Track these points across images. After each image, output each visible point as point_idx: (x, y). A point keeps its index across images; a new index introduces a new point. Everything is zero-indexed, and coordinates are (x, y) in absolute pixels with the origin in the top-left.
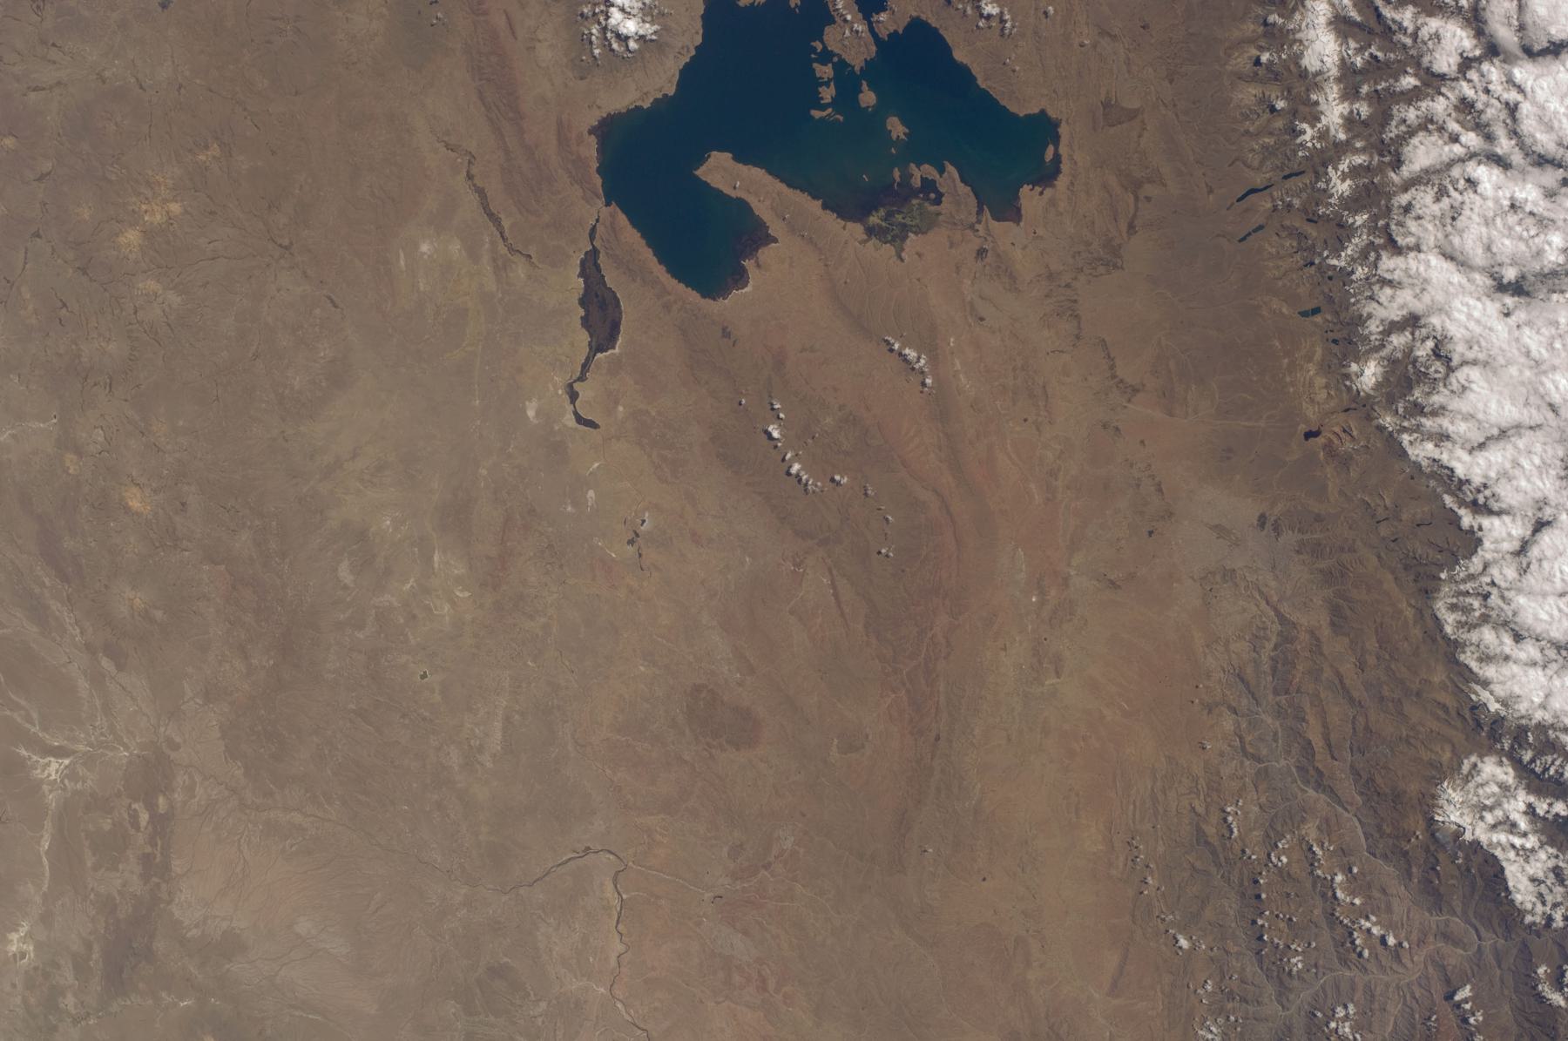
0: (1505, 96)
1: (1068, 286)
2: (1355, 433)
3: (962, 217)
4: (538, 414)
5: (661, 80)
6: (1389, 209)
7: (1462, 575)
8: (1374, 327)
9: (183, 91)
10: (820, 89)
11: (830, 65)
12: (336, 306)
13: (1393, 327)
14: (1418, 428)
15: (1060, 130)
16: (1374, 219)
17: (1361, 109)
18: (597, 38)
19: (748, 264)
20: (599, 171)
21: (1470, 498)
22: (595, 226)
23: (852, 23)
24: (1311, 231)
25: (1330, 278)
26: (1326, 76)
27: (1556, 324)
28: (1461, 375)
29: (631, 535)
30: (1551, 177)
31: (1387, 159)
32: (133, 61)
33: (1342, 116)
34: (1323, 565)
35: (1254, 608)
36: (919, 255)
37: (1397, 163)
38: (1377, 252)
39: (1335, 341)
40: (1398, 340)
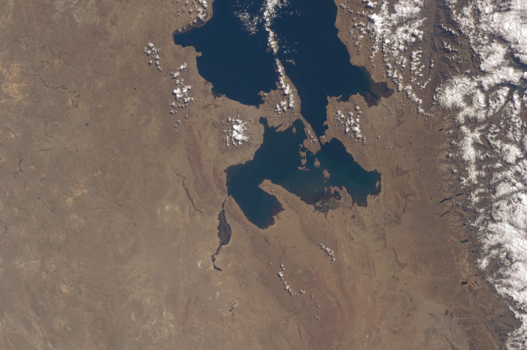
1: (382, 229)
2: (479, 283)
3: (347, 204)
4: (202, 265)
5: (249, 155)
6: (491, 208)
7: (515, 334)
8: (486, 247)
9: (91, 152)
10: (301, 160)
11: (305, 152)
12: (136, 226)
13: (492, 247)
14: (501, 283)
16: (486, 210)
17: (482, 173)
18: (228, 140)
19: (275, 217)
20: (226, 184)
21: (518, 307)
22: (224, 203)
23: (313, 138)
24: (465, 213)
25: (471, 230)
26: (471, 162)
28: (516, 265)
29: (231, 308)
31: (491, 191)
32: (75, 142)
33: (476, 176)
34: (467, 329)
35: (443, 343)
36: (332, 217)
37: (494, 192)
38: (487, 222)
39: (472, 252)
40: (494, 252)
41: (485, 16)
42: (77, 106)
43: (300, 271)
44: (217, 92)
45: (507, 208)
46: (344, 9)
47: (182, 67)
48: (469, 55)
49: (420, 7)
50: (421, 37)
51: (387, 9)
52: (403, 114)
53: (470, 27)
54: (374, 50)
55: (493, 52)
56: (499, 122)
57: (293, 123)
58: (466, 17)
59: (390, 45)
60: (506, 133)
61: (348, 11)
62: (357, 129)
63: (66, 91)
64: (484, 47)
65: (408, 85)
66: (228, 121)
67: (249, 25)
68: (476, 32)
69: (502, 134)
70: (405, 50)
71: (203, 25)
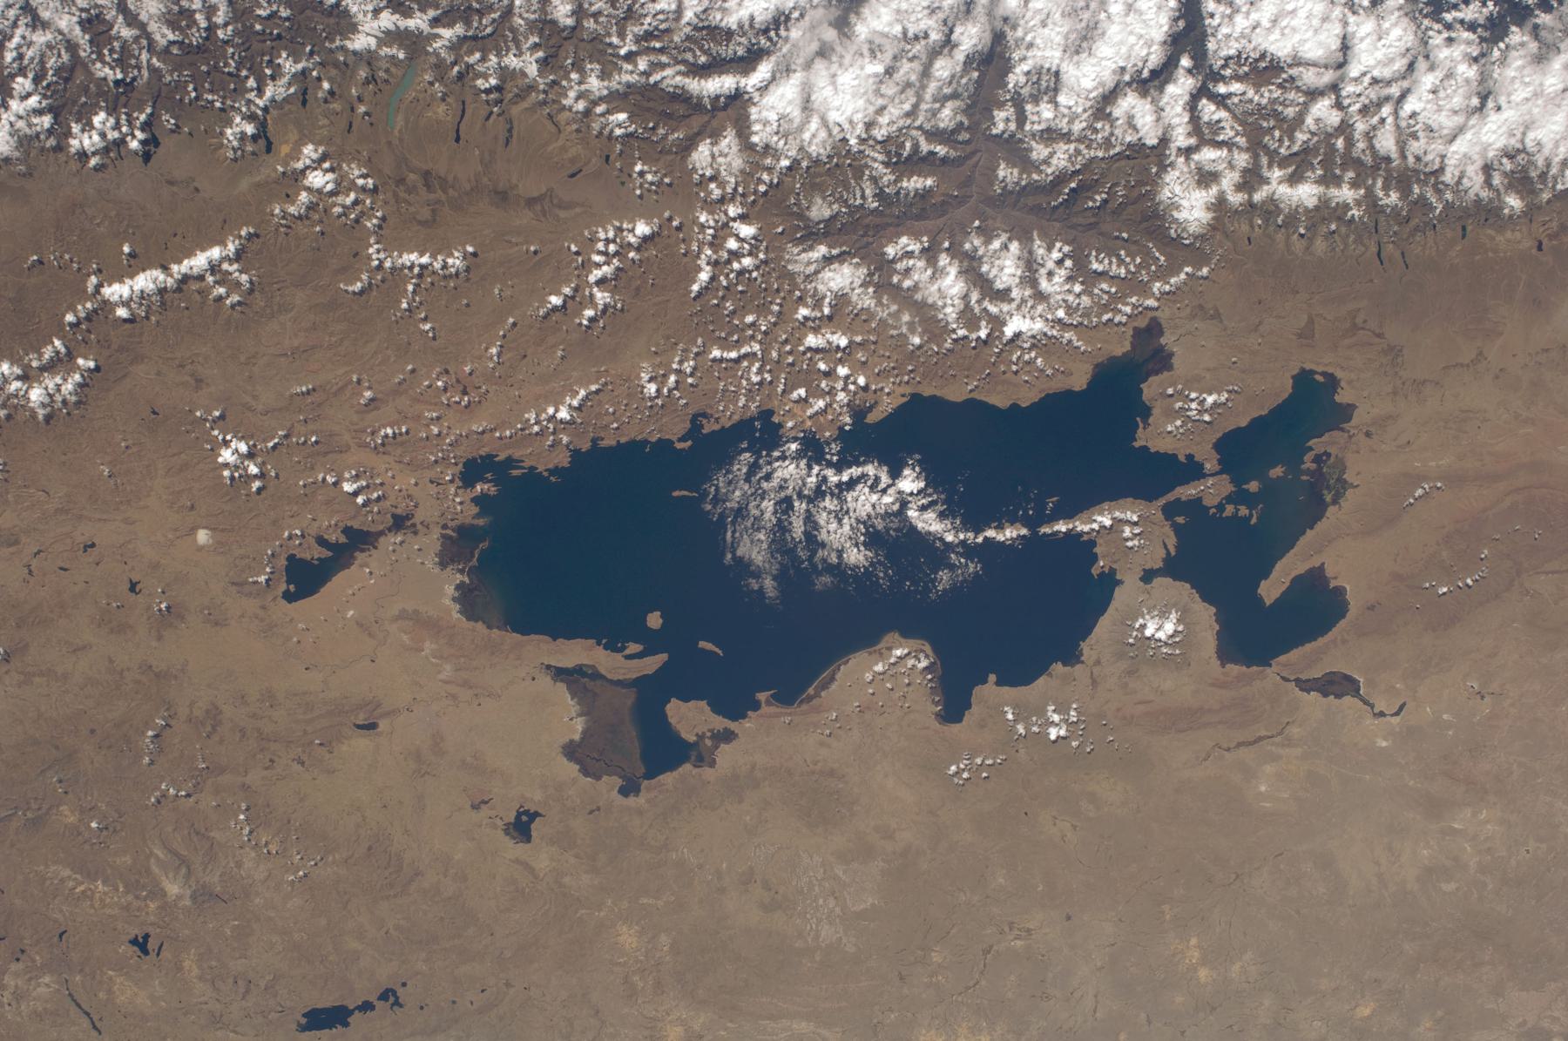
0: (1365, 84)
1: (1404, 383)
2: (1547, 219)
4: (1385, 739)
5: (1205, 614)
6: (1416, 171)
8: (1484, 194)
13: (1488, 183)
16: (1418, 181)
19: (1332, 584)
20: (1248, 667)
24: (1414, 222)
27: (1514, 78)
28: (1529, 144)
30: (1422, 65)
31: (1383, 165)
33: (1350, 189)
36: (1358, 474)
37: (1388, 159)
39: (1486, 220)
40: (1497, 180)
41: (1057, 121)
42: (1029, 931)
43: (1444, 554)
44: (1071, 656)
45: (1423, 141)
46: (976, 387)
47: (1010, 716)
48: (1123, 163)
49: (1010, 239)
50: (1066, 249)
51: (999, 303)
52: (1201, 307)
53: (1071, 151)
54: (1070, 341)
55: (1129, 117)
56: (1262, 128)
57: (1167, 520)
58: (1051, 155)
59: (1070, 310)
60: (1284, 120)
61: (984, 379)
62: (1210, 400)
63: (995, 948)
64: (1116, 132)
65: (1151, 288)
66: (1132, 645)
67: (962, 574)
68: (1083, 143)
69: (1285, 126)
70: (1082, 283)
71: (938, 662)
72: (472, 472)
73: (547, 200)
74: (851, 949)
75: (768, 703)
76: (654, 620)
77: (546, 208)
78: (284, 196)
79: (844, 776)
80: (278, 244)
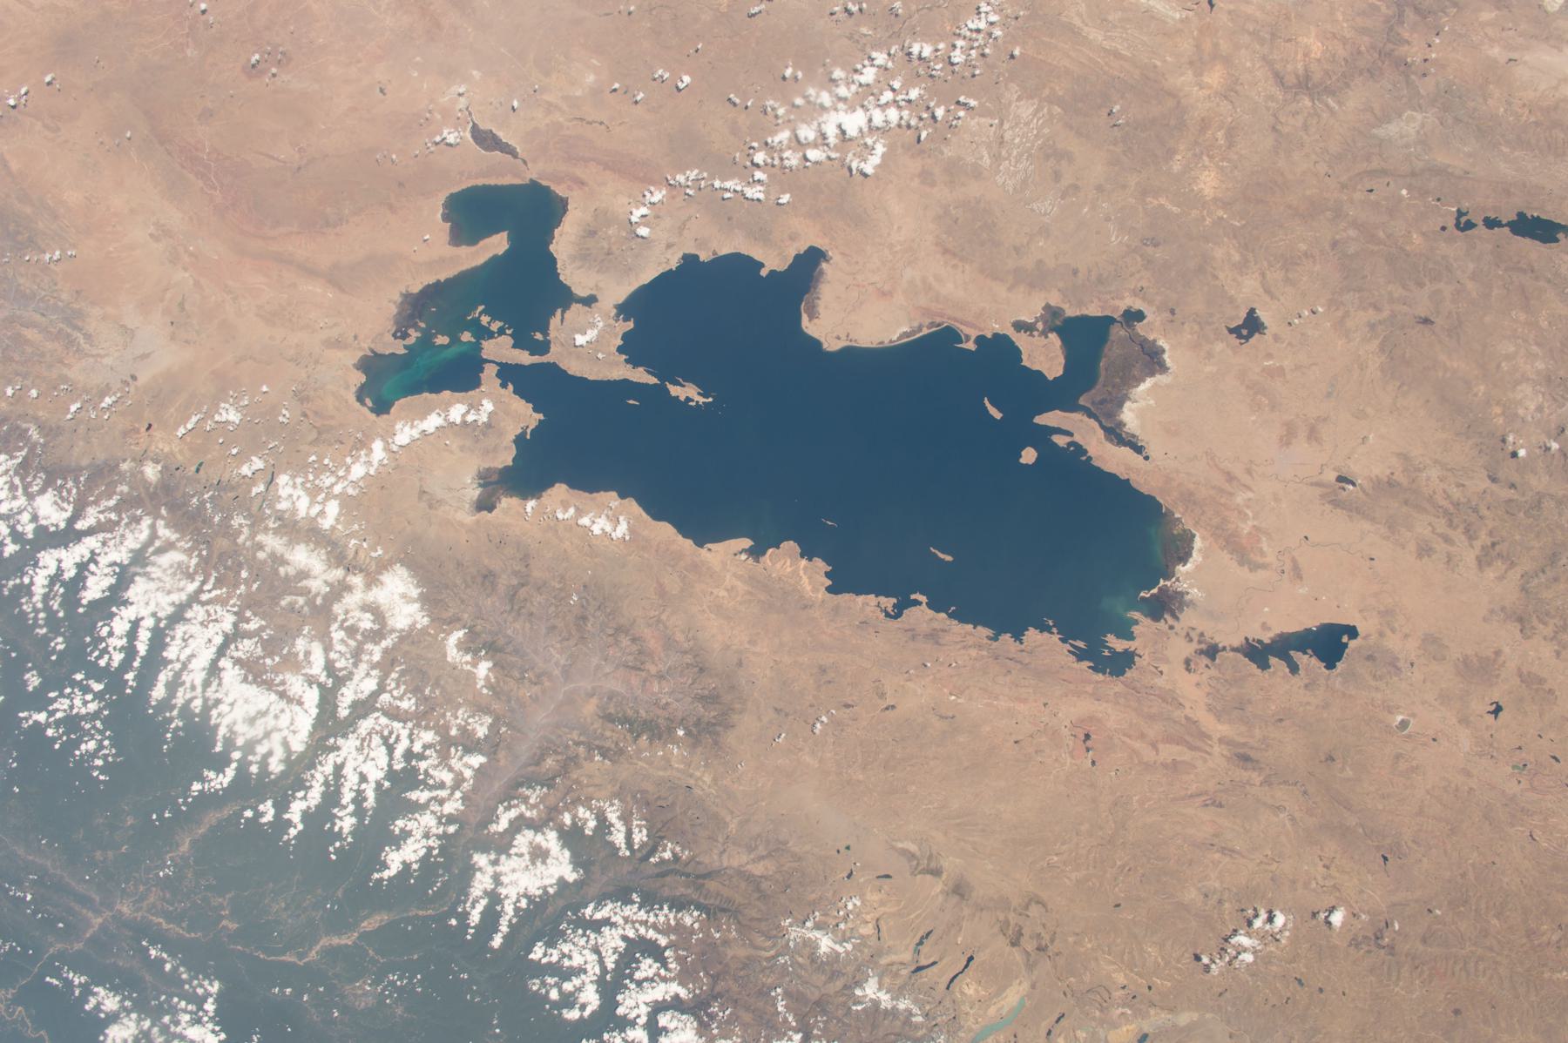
2: (133, 447)
15: (374, 415)
20: (548, 187)
39: (178, 469)
42: (850, 38)
52: (430, 507)
57: (549, 342)
72: (1120, 664)
73: (920, 868)
74: (1014, 87)
75: (968, 338)
76: (1029, 456)
77: (926, 862)
78: (1153, 989)
79: (937, 244)
80: (1184, 949)
